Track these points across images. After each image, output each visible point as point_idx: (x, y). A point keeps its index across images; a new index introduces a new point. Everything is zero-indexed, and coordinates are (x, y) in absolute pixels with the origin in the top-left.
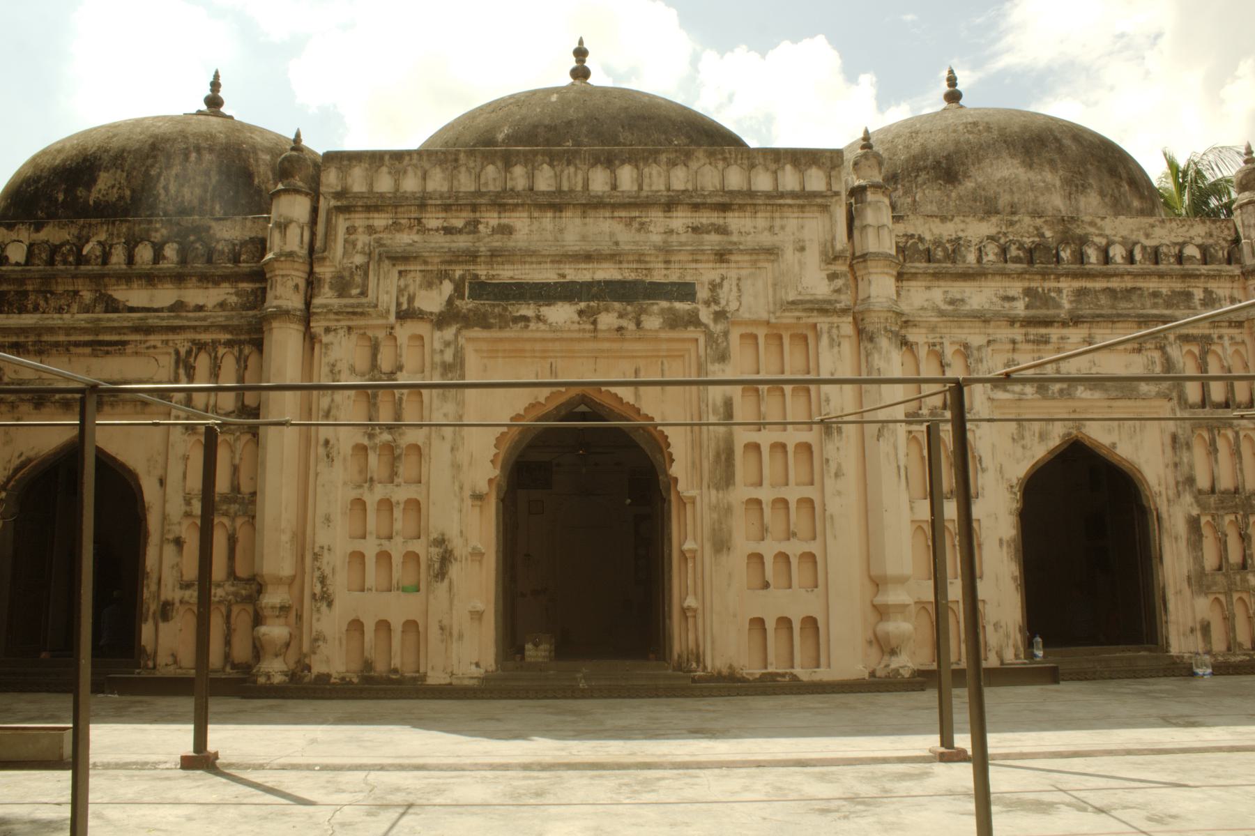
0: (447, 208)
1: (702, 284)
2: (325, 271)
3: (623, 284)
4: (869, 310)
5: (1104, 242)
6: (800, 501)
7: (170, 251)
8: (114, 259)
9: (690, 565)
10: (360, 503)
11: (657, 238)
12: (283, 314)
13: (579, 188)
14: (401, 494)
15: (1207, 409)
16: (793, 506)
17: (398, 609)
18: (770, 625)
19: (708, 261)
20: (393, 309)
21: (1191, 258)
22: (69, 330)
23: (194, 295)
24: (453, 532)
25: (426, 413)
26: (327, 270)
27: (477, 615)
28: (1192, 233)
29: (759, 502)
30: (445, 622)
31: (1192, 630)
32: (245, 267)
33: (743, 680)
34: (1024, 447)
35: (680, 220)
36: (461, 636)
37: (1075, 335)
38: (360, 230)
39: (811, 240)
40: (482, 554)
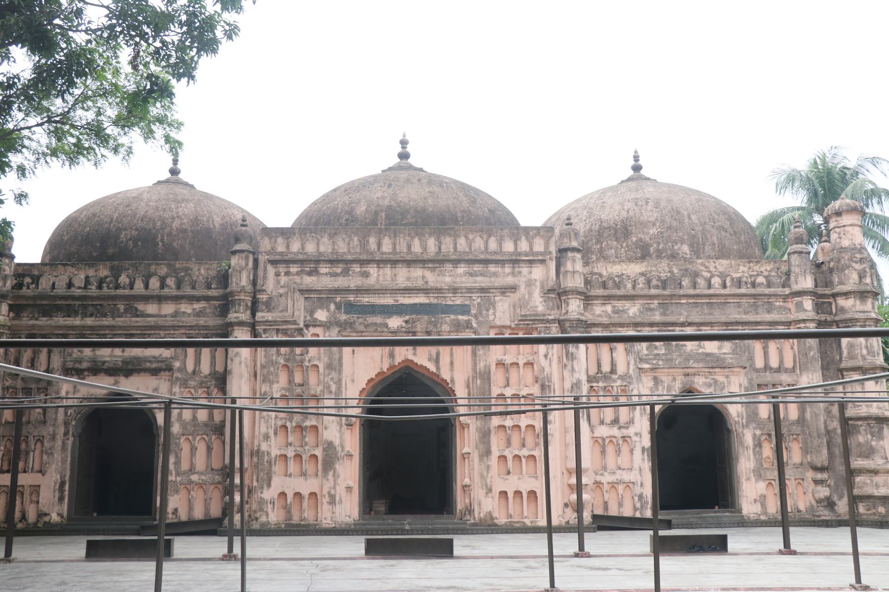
0: (332, 262)
1: (474, 305)
2: (263, 297)
3: (430, 305)
4: (566, 320)
5: (709, 275)
6: (527, 426)
7: (171, 282)
8: (136, 286)
9: (467, 461)
10: (284, 427)
11: (448, 279)
12: (241, 324)
13: (405, 250)
15: (768, 374)
16: (523, 429)
17: (306, 487)
18: (511, 495)
19: (477, 292)
20: (302, 319)
21: (760, 284)
22: (111, 327)
23: (185, 308)
24: (337, 442)
25: (322, 377)
26: (265, 296)
27: (349, 489)
29: (504, 427)
30: (333, 492)
31: (755, 501)
32: (213, 293)
33: (496, 525)
35: (461, 269)
36: (341, 502)
38: (283, 274)
39: (535, 280)
40: (351, 456)
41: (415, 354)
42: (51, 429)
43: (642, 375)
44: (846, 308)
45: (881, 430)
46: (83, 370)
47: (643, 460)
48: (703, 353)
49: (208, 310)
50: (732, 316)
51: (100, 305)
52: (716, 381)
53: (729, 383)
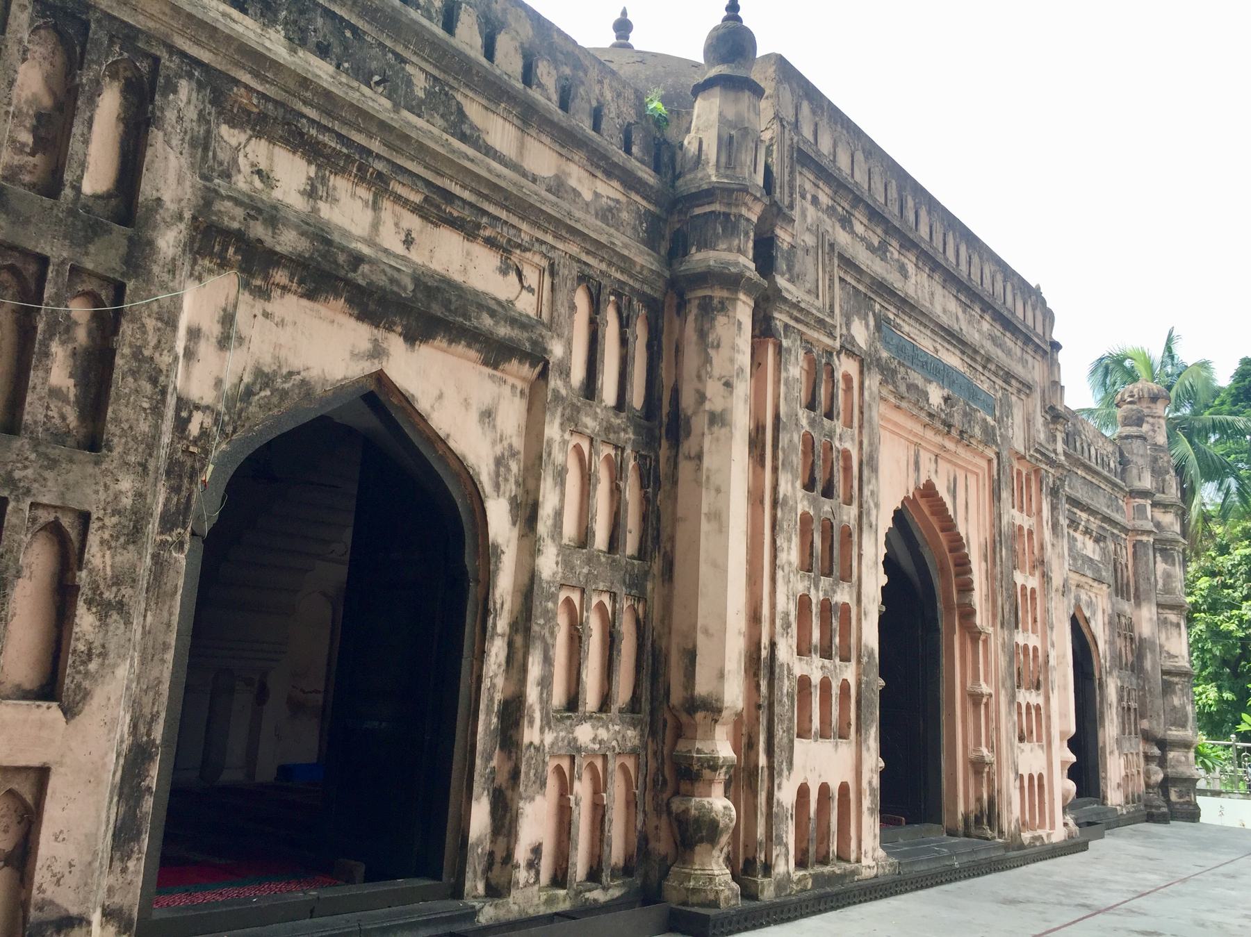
23: (579, 178)
42: (126, 484)
44: (1164, 524)
46: (272, 259)
49: (624, 215)
51: (355, 29)
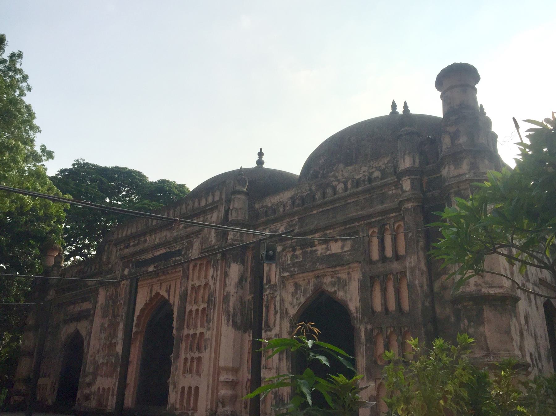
7: (98, 267)
11: (175, 234)
14: (113, 342)
28: (381, 164)
34: (297, 299)
35: (181, 226)
37: (316, 237)
41: (160, 288)
43: (286, 282)
45: (480, 312)
47: (280, 359)
48: (331, 255)
50: (350, 215)
52: (339, 278)
53: (350, 279)
